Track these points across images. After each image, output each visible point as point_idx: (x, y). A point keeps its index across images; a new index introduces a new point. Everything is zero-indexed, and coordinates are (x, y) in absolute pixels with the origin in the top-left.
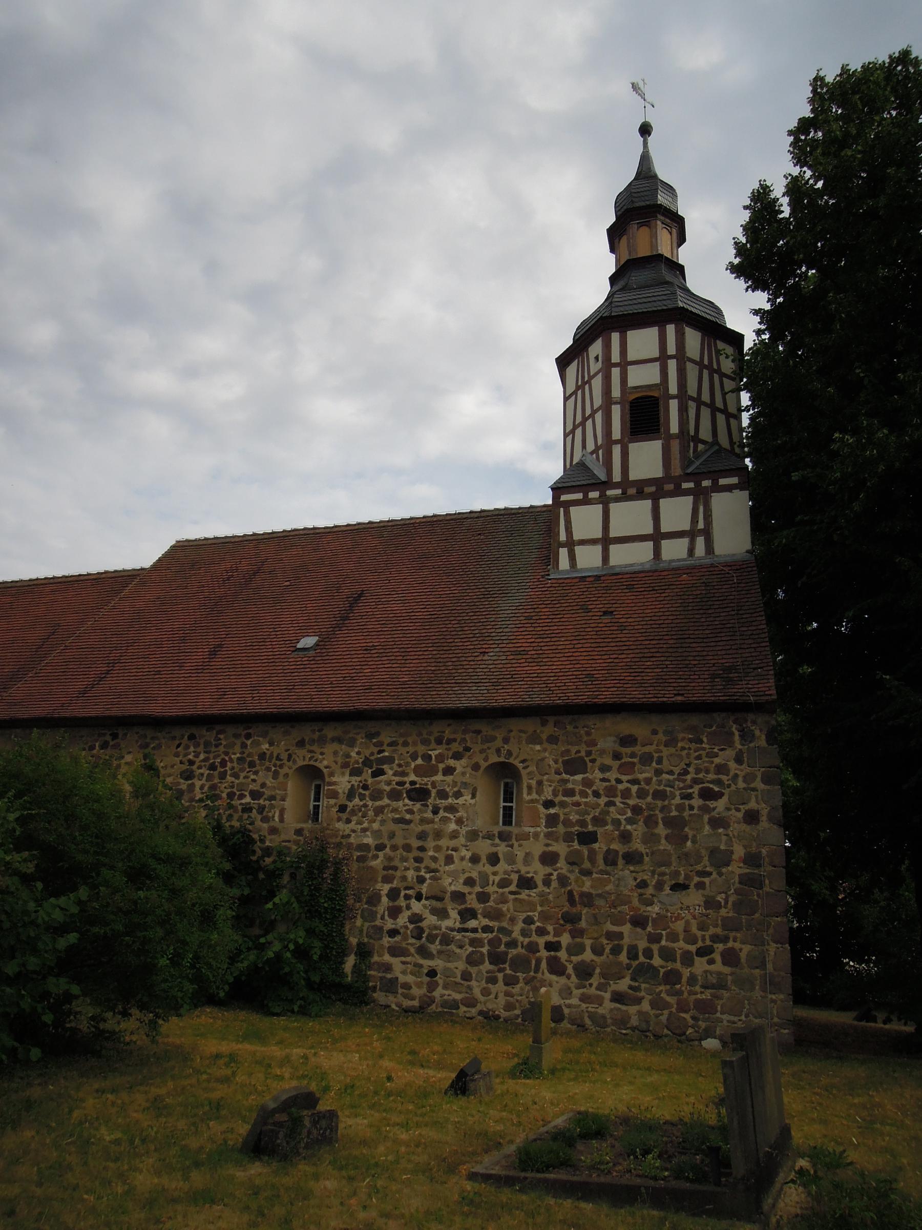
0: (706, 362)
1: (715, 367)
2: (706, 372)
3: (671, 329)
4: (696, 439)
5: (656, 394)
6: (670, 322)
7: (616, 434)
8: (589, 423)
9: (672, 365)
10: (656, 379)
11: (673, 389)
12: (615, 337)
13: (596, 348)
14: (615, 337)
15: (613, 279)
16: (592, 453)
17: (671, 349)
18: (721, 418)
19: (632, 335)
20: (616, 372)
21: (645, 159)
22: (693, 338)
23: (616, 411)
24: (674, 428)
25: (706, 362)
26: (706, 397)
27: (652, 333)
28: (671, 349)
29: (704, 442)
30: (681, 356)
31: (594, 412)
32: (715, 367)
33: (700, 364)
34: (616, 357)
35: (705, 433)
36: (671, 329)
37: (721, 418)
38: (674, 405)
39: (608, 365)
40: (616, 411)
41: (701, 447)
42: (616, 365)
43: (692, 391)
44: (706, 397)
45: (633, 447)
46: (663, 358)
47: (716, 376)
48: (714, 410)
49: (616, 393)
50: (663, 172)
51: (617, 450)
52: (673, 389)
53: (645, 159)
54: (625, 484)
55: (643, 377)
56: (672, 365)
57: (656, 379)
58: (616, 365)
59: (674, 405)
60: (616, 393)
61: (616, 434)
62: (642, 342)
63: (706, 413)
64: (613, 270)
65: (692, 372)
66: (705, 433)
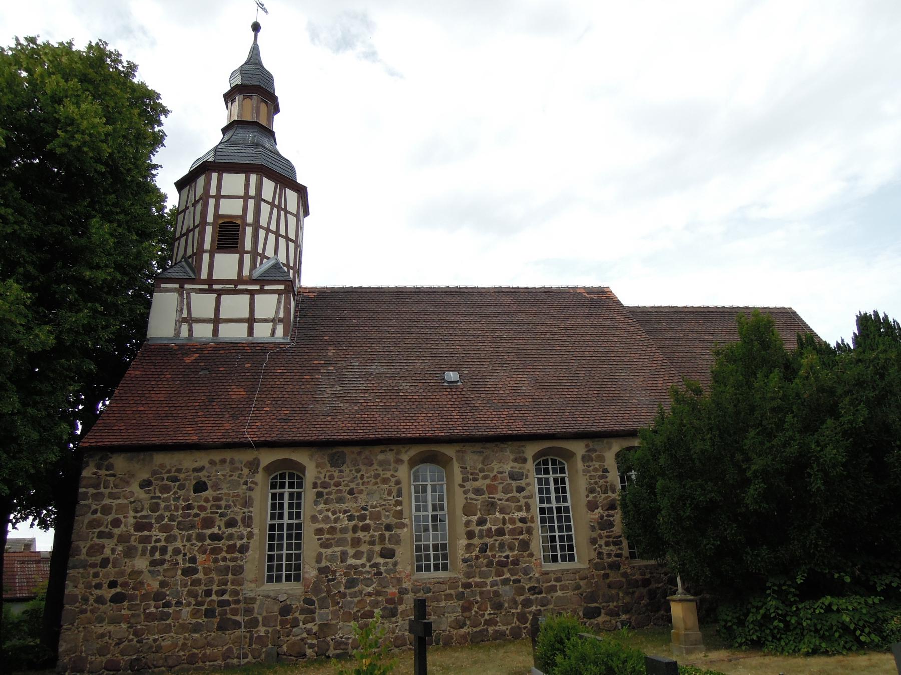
0: (276, 203)
1: (283, 207)
2: (275, 210)
4: (264, 257)
5: (239, 222)
6: (253, 173)
7: (207, 246)
8: (191, 235)
9: (251, 203)
10: (239, 212)
11: (250, 219)
12: (215, 176)
13: (201, 181)
14: (215, 176)
15: (225, 131)
16: (189, 258)
17: (252, 193)
18: (282, 242)
19: (226, 176)
20: (212, 202)
21: (255, 52)
22: (269, 187)
23: (209, 230)
24: (248, 247)
25: (276, 203)
26: (273, 227)
27: (241, 178)
28: (252, 193)
29: (268, 258)
31: (195, 227)
32: (283, 207)
33: (272, 205)
34: (213, 192)
35: (270, 252)
36: (253, 178)
37: (282, 242)
38: (249, 231)
40: (209, 230)
41: (265, 260)
42: (213, 197)
43: (263, 222)
44: (273, 227)
45: (218, 257)
46: (246, 197)
47: (283, 213)
48: (278, 235)
49: (210, 218)
50: (268, 63)
51: (206, 257)
52: (250, 219)
53: (255, 52)
54: (210, 281)
55: (231, 208)
56: (251, 203)
57: (239, 212)
58: (213, 197)
59: (249, 231)
60: (210, 218)
61: (207, 246)
62: (233, 183)
63: (272, 237)
64: (225, 124)
65: (265, 209)
66: (270, 252)
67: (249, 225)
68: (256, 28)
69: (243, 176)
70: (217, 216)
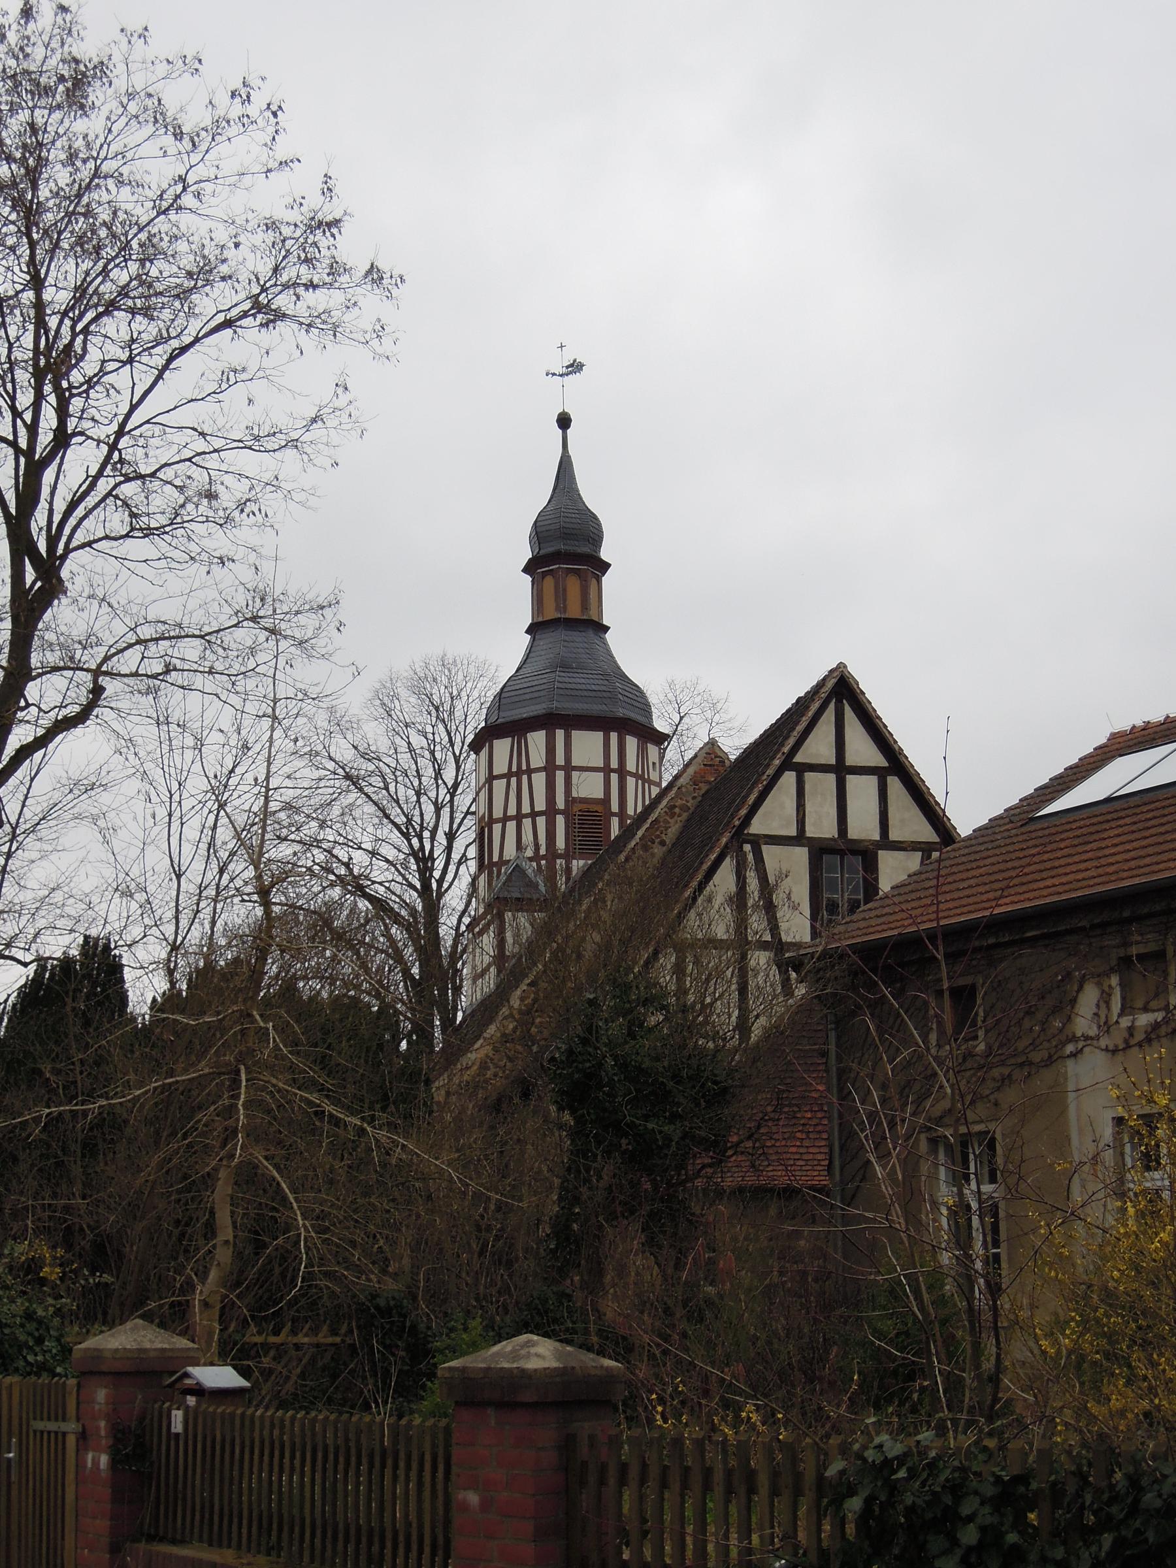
3: (614, 736)
5: (599, 808)
10: (600, 794)
11: (615, 807)
12: (560, 734)
14: (560, 734)
17: (614, 764)
20: (560, 776)
21: (565, 469)
23: (560, 820)
30: (622, 772)
39: (550, 768)
42: (560, 768)
46: (606, 770)
49: (560, 804)
52: (615, 807)
53: (565, 469)
55: (589, 787)
57: (600, 794)
60: (560, 804)
65: (631, 781)
67: (615, 814)
68: (564, 422)
69: (600, 735)
70: (570, 800)
